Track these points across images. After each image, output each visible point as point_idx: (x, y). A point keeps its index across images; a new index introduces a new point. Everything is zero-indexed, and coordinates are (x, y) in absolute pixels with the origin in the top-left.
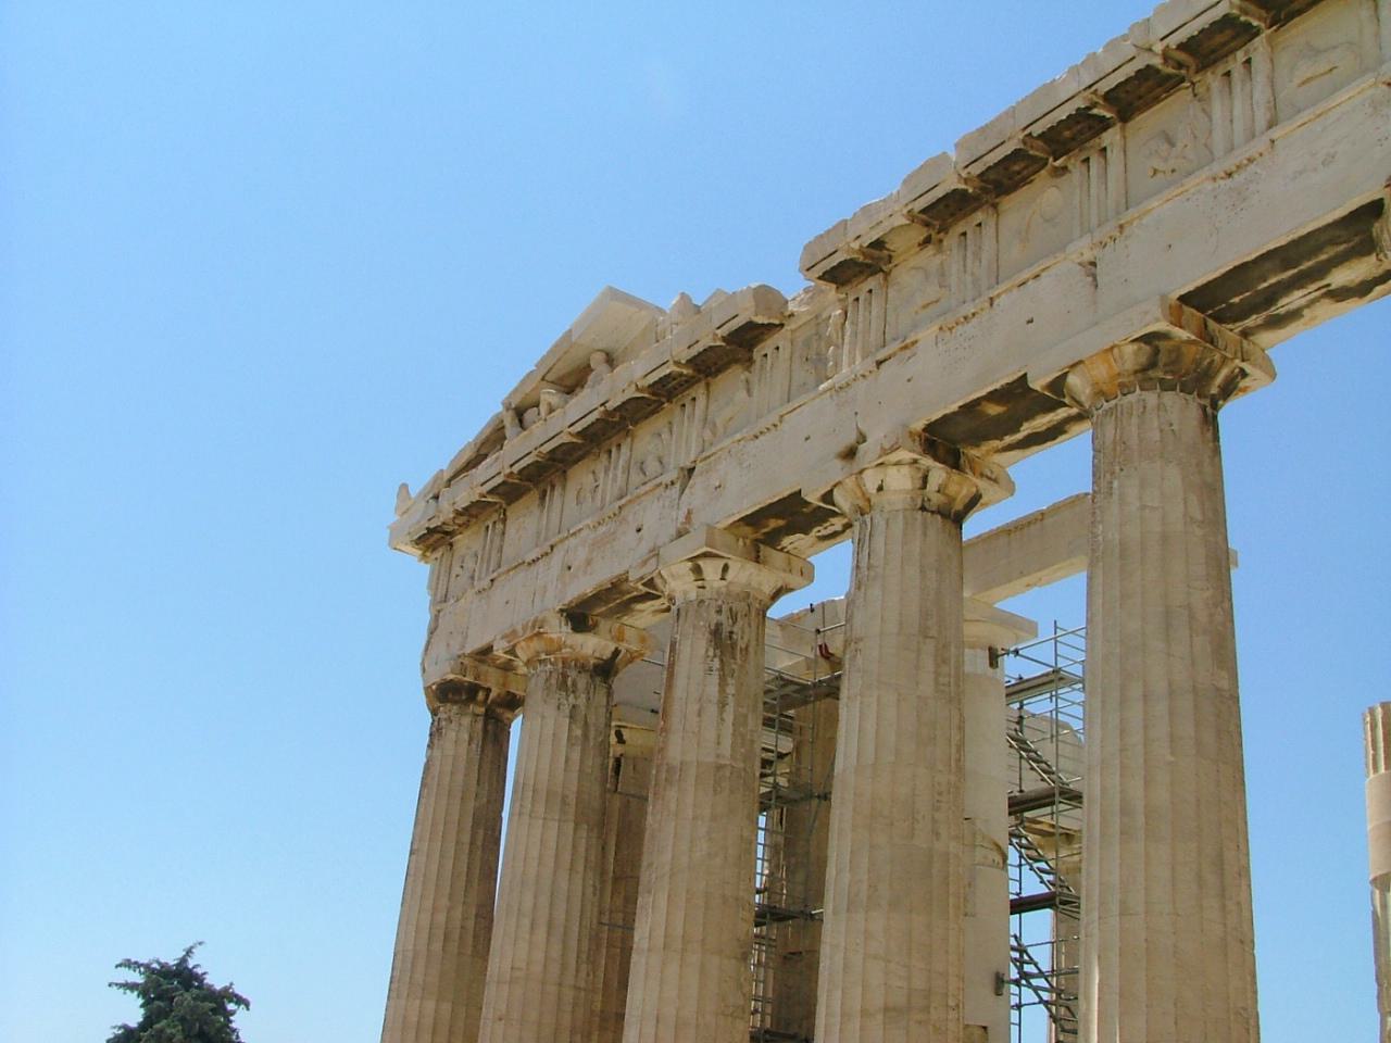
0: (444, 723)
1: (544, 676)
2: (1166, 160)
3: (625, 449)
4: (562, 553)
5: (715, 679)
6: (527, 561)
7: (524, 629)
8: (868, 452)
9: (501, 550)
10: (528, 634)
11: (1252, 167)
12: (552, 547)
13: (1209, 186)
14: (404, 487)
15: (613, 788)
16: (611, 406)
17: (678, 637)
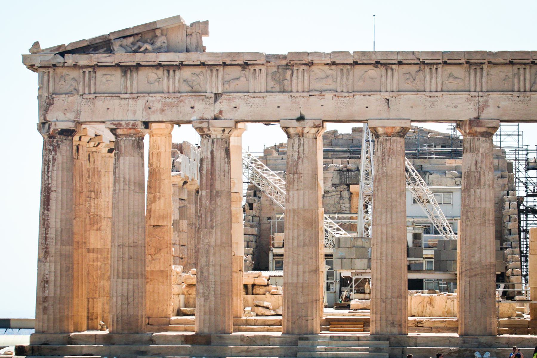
0: (60, 143)
1: (131, 142)
2: (412, 82)
3: (177, 73)
4: (144, 102)
5: (226, 165)
6: (122, 97)
7: (128, 124)
8: (308, 123)
9: (95, 84)
10: (130, 127)
11: (436, 98)
12: (138, 97)
13: (424, 97)
14: (37, 44)
15: (76, 158)
17: (214, 150)
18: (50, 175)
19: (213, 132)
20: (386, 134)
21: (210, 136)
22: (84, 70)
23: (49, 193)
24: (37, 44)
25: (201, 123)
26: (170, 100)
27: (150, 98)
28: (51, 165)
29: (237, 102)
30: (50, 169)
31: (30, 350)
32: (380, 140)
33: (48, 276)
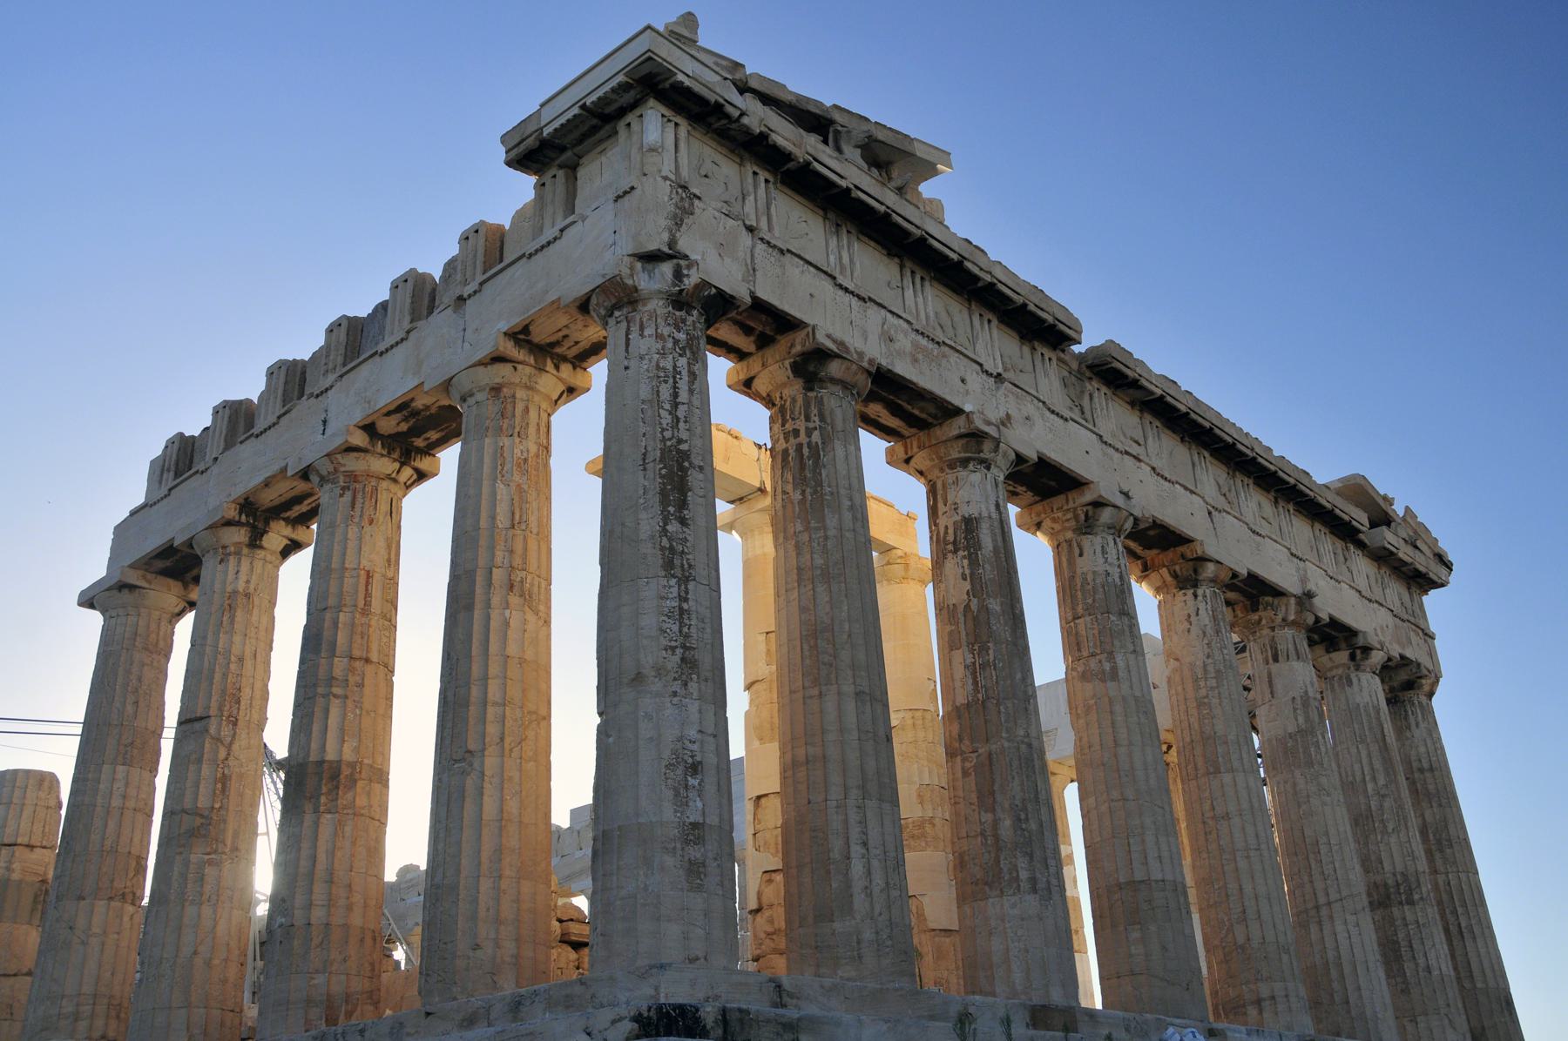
10: (865, 364)
14: (690, 19)
16: (967, 264)
18: (681, 411)
19: (999, 458)
20: (1214, 581)
21: (988, 468)
22: (756, 169)
23: (684, 470)
24: (690, 19)
25: (989, 423)
26: (924, 342)
27: (889, 315)
28: (683, 385)
29: (1030, 408)
30: (683, 396)
31: (716, 1022)
32: (1200, 592)
33: (695, 747)
